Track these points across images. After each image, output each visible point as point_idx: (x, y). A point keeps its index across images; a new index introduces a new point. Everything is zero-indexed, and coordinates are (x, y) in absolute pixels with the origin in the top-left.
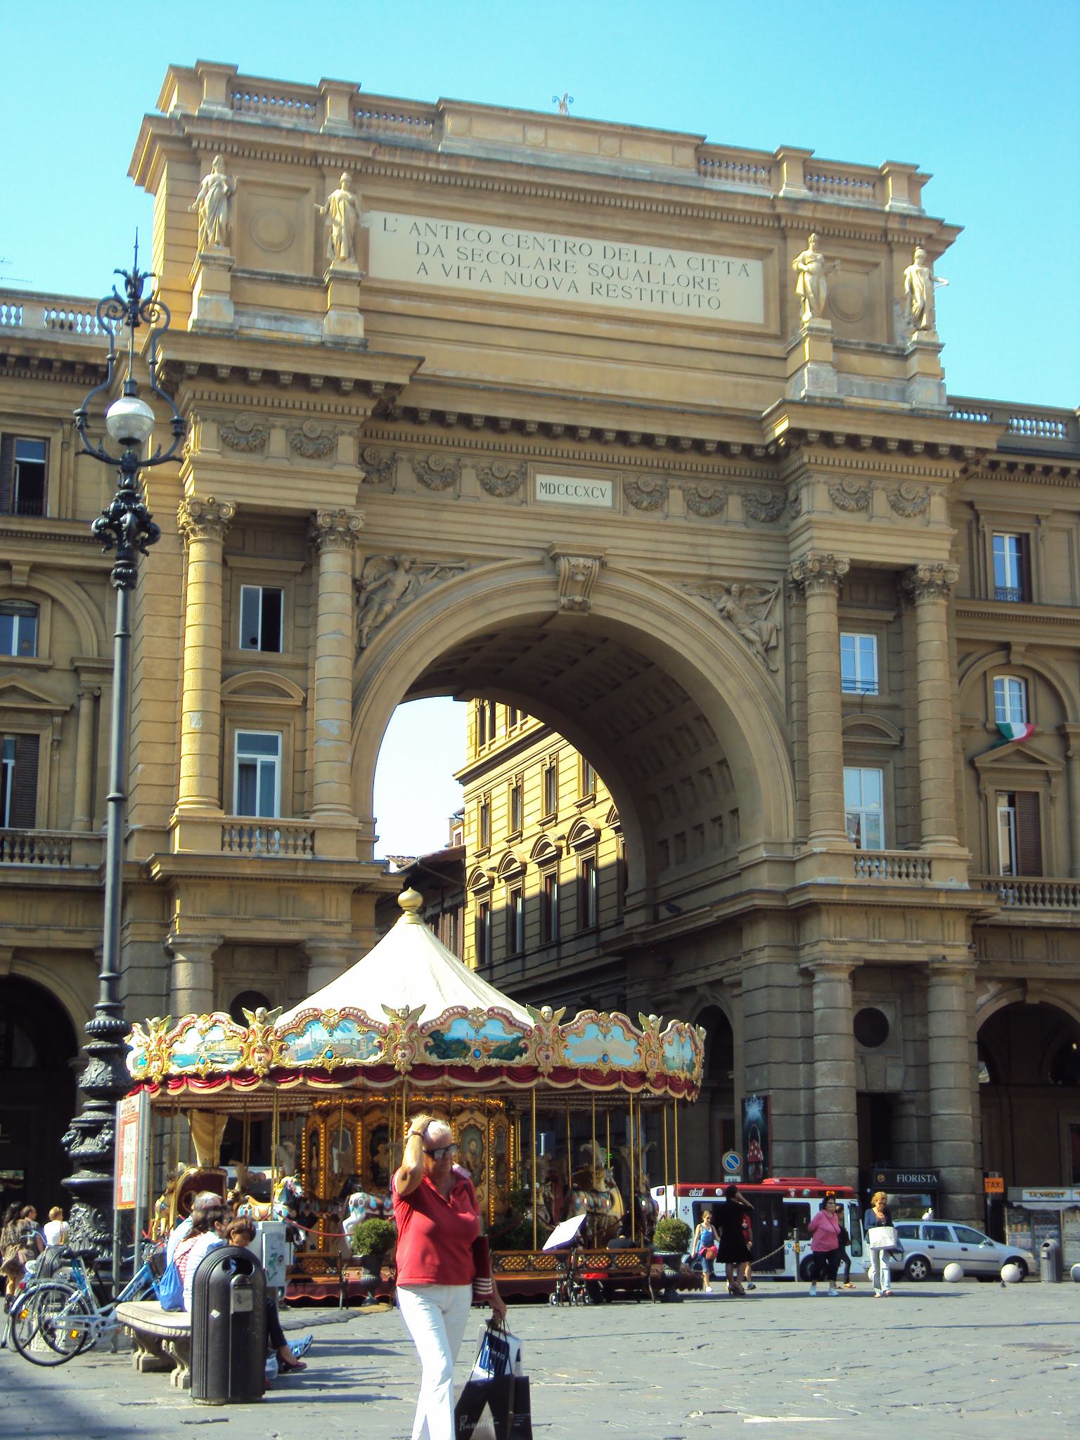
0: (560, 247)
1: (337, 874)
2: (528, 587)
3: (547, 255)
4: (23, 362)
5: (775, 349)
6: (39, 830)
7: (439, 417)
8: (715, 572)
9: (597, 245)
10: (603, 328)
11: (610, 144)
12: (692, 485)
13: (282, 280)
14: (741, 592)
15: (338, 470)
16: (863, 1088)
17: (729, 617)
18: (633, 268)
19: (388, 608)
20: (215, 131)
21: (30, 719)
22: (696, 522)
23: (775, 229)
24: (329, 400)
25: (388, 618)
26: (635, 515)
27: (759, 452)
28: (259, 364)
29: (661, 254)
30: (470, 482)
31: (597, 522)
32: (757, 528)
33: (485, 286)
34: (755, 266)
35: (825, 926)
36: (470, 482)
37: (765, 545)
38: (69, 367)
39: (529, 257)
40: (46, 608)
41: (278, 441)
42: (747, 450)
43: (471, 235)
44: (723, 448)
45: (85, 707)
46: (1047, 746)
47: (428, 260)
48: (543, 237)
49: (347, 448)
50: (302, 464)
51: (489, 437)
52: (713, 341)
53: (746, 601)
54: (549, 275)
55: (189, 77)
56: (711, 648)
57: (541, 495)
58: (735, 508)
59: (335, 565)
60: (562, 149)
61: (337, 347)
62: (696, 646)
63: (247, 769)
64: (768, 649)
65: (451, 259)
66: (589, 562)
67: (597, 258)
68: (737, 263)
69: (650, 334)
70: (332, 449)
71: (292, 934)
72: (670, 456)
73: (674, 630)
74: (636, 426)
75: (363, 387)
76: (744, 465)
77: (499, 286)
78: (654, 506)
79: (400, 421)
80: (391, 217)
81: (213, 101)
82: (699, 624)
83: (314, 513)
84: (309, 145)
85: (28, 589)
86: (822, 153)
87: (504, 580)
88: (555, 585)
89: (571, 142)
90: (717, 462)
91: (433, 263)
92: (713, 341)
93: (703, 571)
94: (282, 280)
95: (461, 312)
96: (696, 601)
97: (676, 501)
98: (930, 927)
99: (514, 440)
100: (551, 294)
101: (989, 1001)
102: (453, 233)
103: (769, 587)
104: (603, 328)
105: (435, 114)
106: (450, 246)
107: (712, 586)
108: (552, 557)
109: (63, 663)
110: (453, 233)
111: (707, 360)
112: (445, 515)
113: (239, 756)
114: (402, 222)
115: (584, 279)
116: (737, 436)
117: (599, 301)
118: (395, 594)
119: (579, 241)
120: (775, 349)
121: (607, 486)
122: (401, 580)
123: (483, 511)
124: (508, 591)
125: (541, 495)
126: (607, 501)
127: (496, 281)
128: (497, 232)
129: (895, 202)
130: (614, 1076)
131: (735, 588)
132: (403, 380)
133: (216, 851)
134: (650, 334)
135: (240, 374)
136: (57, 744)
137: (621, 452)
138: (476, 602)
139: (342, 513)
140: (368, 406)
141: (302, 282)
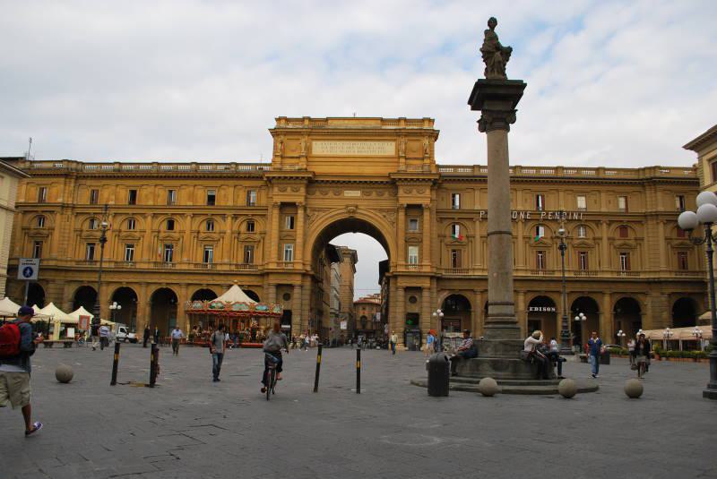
5: (396, 160)
11: (362, 122)
16: (409, 311)
17: (385, 216)
23: (396, 134)
26: (365, 197)
29: (373, 143)
30: (331, 194)
34: (394, 143)
35: (399, 279)
36: (331, 194)
42: (387, 182)
44: (382, 182)
46: (464, 240)
49: (303, 190)
55: (278, 120)
56: (380, 223)
57: (346, 195)
59: (300, 212)
60: (352, 125)
61: (299, 171)
63: (287, 251)
68: (389, 143)
71: (289, 283)
75: (303, 178)
81: (283, 124)
86: (408, 118)
87: (336, 213)
89: (354, 122)
90: (382, 186)
97: (374, 193)
98: (422, 280)
101: (446, 294)
105: (327, 119)
106: (329, 147)
108: (347, 206)
114: (319, 143)
120: (396, 160)
122: (316, 213)
125: (346, 195)
126: (359, 195)
127: (338, 153)
129: (426, 126)
130: (242, 312)
132: (310, 176)
139: (301, 203)
141: (297, 158)
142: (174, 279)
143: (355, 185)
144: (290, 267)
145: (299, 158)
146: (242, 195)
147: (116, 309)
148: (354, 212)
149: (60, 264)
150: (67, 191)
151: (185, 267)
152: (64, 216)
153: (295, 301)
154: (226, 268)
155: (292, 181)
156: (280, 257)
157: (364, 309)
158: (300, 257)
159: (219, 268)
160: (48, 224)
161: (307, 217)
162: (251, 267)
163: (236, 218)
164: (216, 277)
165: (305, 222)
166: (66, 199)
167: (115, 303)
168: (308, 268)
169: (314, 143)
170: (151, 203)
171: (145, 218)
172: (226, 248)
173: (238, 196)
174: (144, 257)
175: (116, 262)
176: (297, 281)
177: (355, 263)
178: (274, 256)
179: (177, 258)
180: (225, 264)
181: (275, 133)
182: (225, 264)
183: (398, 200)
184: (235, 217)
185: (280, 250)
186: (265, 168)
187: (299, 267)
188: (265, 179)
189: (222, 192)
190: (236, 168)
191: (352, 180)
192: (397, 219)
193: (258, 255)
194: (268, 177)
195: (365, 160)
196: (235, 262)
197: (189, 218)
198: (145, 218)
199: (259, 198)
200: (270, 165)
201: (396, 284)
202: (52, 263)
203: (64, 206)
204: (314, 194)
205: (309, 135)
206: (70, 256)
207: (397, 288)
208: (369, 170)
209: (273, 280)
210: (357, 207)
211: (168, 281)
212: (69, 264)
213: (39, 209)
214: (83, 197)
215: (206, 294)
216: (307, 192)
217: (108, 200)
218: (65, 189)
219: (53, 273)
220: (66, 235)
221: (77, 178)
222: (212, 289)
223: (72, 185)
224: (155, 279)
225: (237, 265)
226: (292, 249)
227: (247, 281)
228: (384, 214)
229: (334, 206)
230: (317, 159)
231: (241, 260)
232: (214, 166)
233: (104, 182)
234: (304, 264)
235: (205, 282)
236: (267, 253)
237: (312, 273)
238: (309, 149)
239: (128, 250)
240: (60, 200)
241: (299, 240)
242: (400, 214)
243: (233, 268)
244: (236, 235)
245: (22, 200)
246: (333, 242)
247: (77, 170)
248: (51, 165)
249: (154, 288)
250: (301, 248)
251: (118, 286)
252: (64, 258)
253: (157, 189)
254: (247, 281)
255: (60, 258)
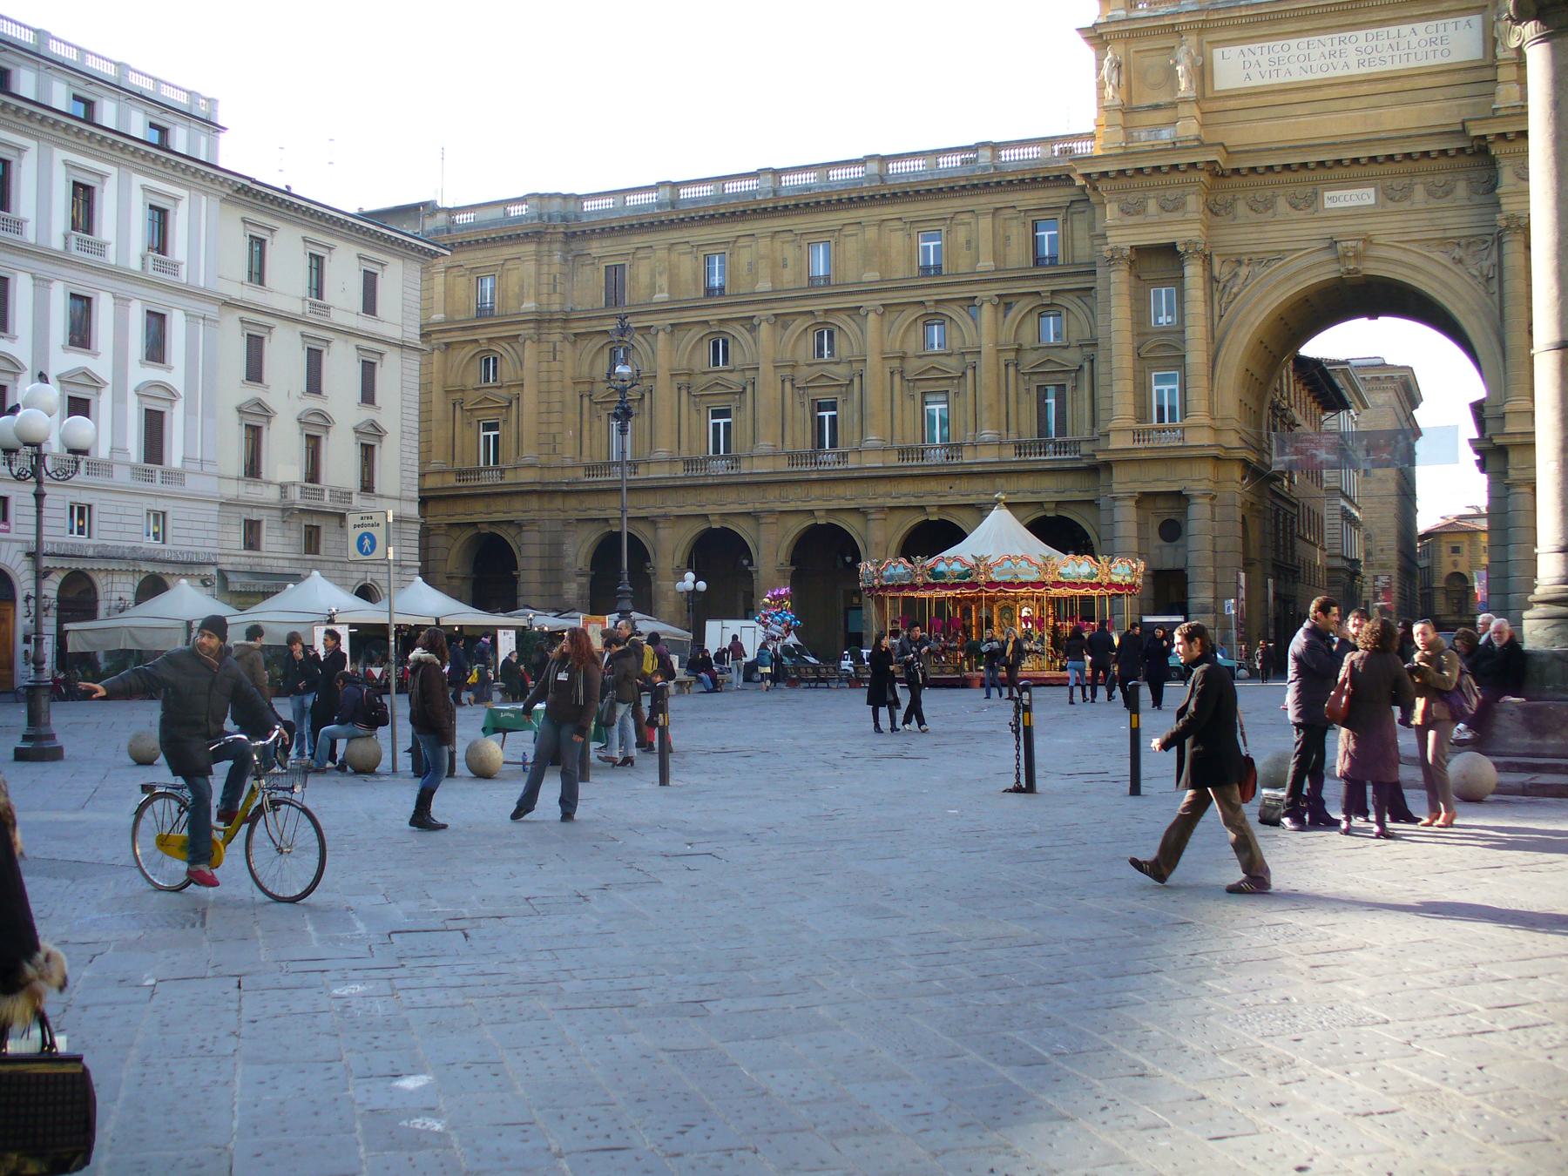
0: (1336, 42)
1: (1194, 453)
2: (1321, 264)
3: (1326, 51)
4: (1034, 180)
6: (1069, 438)
7: (1253, 170)
8: (1449, 234)
9: (1361, 34)
10: (1364, 89)
12: (1430, 179)
13: (1156, 107)
14: (1469, 244)
15: (1188, 216)
17: (1460, 261)
18: (1387, 42)
19: (1235, 290)
20: (1114, 28)
21: (1060, 376)
22: (1434, 203)
24: (1176, 177)
25: (1236, 295)
26: (1391, 206)
27: (1469, 151)
28: (1130, 166)
29: (1405, 29)
30: (1282, 205)
31: (1364, 215)
32: (1478, 199)
33: (1288, 79)
36: (1282, 205)
37: (1484, 210)
38: (1058, 178)
39: (1315, 53)
40: (1064, 312)
41: (1152, 205)
42: (1461, 151)
43: (1278, 48)
44: (1444, 152)
45: (1087, 366)
47: (1251, 71)
48: (1325, 38)
50: (1167, 216)
51: (1287, 176)
52: (1442, 80)
53: (1473, 249)
54: (1328, 61)
57: (1328, 205)
58: (1461, 189)
59: (1193, 272)
62: (1436, 285)
64: (1489, 279)
65: (1265, 67)
66: (1353, 244)
67: (1362, 43)
69: (1396, 86)
70: (1184, 204)
72: (1409, 165)
73: (1420, 277)
74: (1380, 152)
75: (1193, 165)
76: (1463, 160)
77: (1298, 76)
78: (1407, 197)
79: (1226, 177)
80: (1226, 50)
82: (1437, 271)
83: (1173, 245)
84: (1167, 21)
85: (1052, 305)
87: (1303, 263)
88: (1338, 260)
91: (1253, 72)
92: (1442, 80)
93: (1439, 235)
94: (1156, 107)
95: (1270, 99)
96: (1437, 256)
97: (1419, 192)
99: (1304, 174)
100: (1332, 73)
102: (1265, 50)
103: (1489, 238)
104: (1364, 89)
106: (1264, 60)
107: (1443, 241)
108: (1333, 244)
109: (1074, 343)
110: (1265, 50)
111: (1439, 94)
112: (1268, 228)
113: (1155, 388)
114: (1233, 51)
115: (1353, 58)
116: (1451, 145)
117: (1364, 70)
118: (1240, 281)
119: (1348, 34)
121: (1371, 191)
123: (1291, 221)
124: (1308, 268)
125: (1328, 205)
127: (1295, 73)
128: (1293, 42)
130: (1023, 585)
131: (1463, 242)
133: (1131, 446)
134: (1396, 86)
135: (1122, 172)
136: (1075, 388)
137: (1375, 169)
138: (1288, 279)
140: (1204, 177)
142: (844, 496)
143: (1356, 170)
144: (1169, 440)
145: (1173, 105)
146: (1018, 234)
147: (694, 592)
148: (1358, 256)
149: (549, 477)
150: (544, 279)
151: (872, 461)
152: (545, 347)
153: (1193, 543)
154: (988, 455)
155: (1157, 180)
156: (1142, 416)
157: (1456, 550)
158: (1207, 406)
159: (968, 456)
160: (507, 371)
161: (1212, 280)
162: (1061, 447)
163: (1008, 306)
164: (963, 485)
165: (1210, 300)
166: (544, 298)
167: (690, 576)
168: (1232, 440)
169: (1217, 52)
170: (764, 285)
171: (753, 329)
172: (987, 396)
173: (1008, 238)
174: (769, 440)
175: (689, 462)
176: (1196, 480)
177: (1415, 405)
178: (1122, 410)
179: (847, 435)
180: (986, 444)
181: (1096, 36)
182: (986, 444)
183: (1497, 205)
184: (1005, 303)
185: (1142, 390)
186: (1081, 148)
187: (1200, 438)
188: (1080, 182)
189: (961, 234)
190: (996, 156)
191: (1348, 155)
192: (1500, 265)
193: (1079, 407)
194: (1087, 176)
195: (1382, 87)
196: (1013, 437)
197: (872, 316)
198: (750, 323)
199: (1068, 238)
200: (1091, 136)
201: (1505, 473)
202: (527, 476)
203: (541, 321)
204: (1229, 207)
205: (1201, 31)
206: (569, 453)
207: (1508, 487)
208: (1397, 118)
209: (1124, 482)
210: (1368, 241)
211: (834, 504)
212: (569, 475)
213: (481, 335)
214: (588, 290)
215: (936, 535)
216: (1212, 210)
217: (652, 288)
218: (539, 274)
219: (534, 503)
220: (556, 397)
221: (570, 236)
222: (956, 518)
223: (557, 258)
224: (795, 499)
225: (1019, 447)
226: (1176, 387)
227: (1049, 491)
228: (1458, 253)
229: (1293, 244)
230: (1231, 104)
231: (1029, 432)
232: (932, 160)
233: (638, 240)
234: (1216, 430)
235: (933, 500)
236: (1102, 404)
237: (1243, 454)
238: (1203, 73)
239: (716, 426)
240: (529, 305)
241: (1196, 356)
242: (1507, 248)
243: (1009, 454)
244: (1012, 355)
245: (438, 316)
246: (1313, 349)
247: (564, 219)
248: (497, 213)
249: (797, 526)
250: (1204, 382)
251: (702, 526)
252: (555, 461)
253: (777, 244)
254: (1025, 489)
255: (544, 459)
